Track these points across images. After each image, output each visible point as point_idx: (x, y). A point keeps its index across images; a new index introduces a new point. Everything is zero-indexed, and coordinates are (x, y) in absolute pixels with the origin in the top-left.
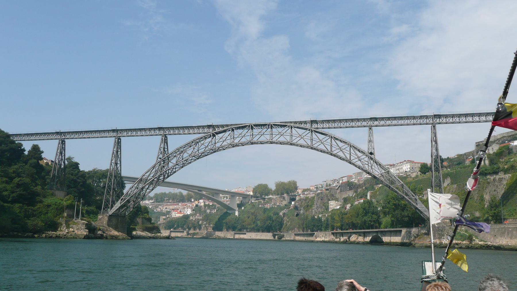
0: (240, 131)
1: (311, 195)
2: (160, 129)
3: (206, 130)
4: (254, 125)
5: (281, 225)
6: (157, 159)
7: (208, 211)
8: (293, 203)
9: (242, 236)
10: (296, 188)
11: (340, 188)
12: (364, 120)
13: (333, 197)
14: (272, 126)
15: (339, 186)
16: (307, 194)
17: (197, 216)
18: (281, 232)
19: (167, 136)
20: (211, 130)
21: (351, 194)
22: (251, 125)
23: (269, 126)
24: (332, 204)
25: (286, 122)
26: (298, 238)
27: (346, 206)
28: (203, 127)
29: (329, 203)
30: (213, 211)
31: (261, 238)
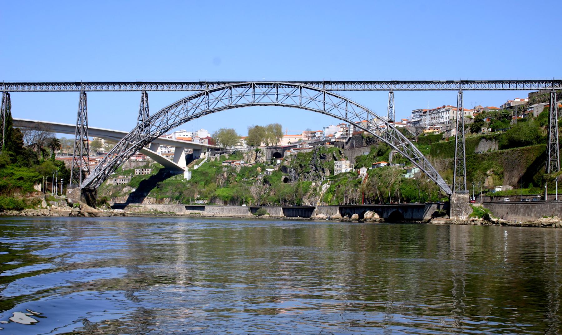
0: (240, 90)
3: (197, 87)
4: (256, 84)
6: (138, 123)
7: (138, 171)
15: (350, 139)
16: (300, 149)
17: (119, 180)
19: (146, 92)
20: (203, 88)
22: (253, 83)
23: (275, 85)
27: (360, 170)
29: (335, 163)
30: (146, 172)
31: (229, 214)
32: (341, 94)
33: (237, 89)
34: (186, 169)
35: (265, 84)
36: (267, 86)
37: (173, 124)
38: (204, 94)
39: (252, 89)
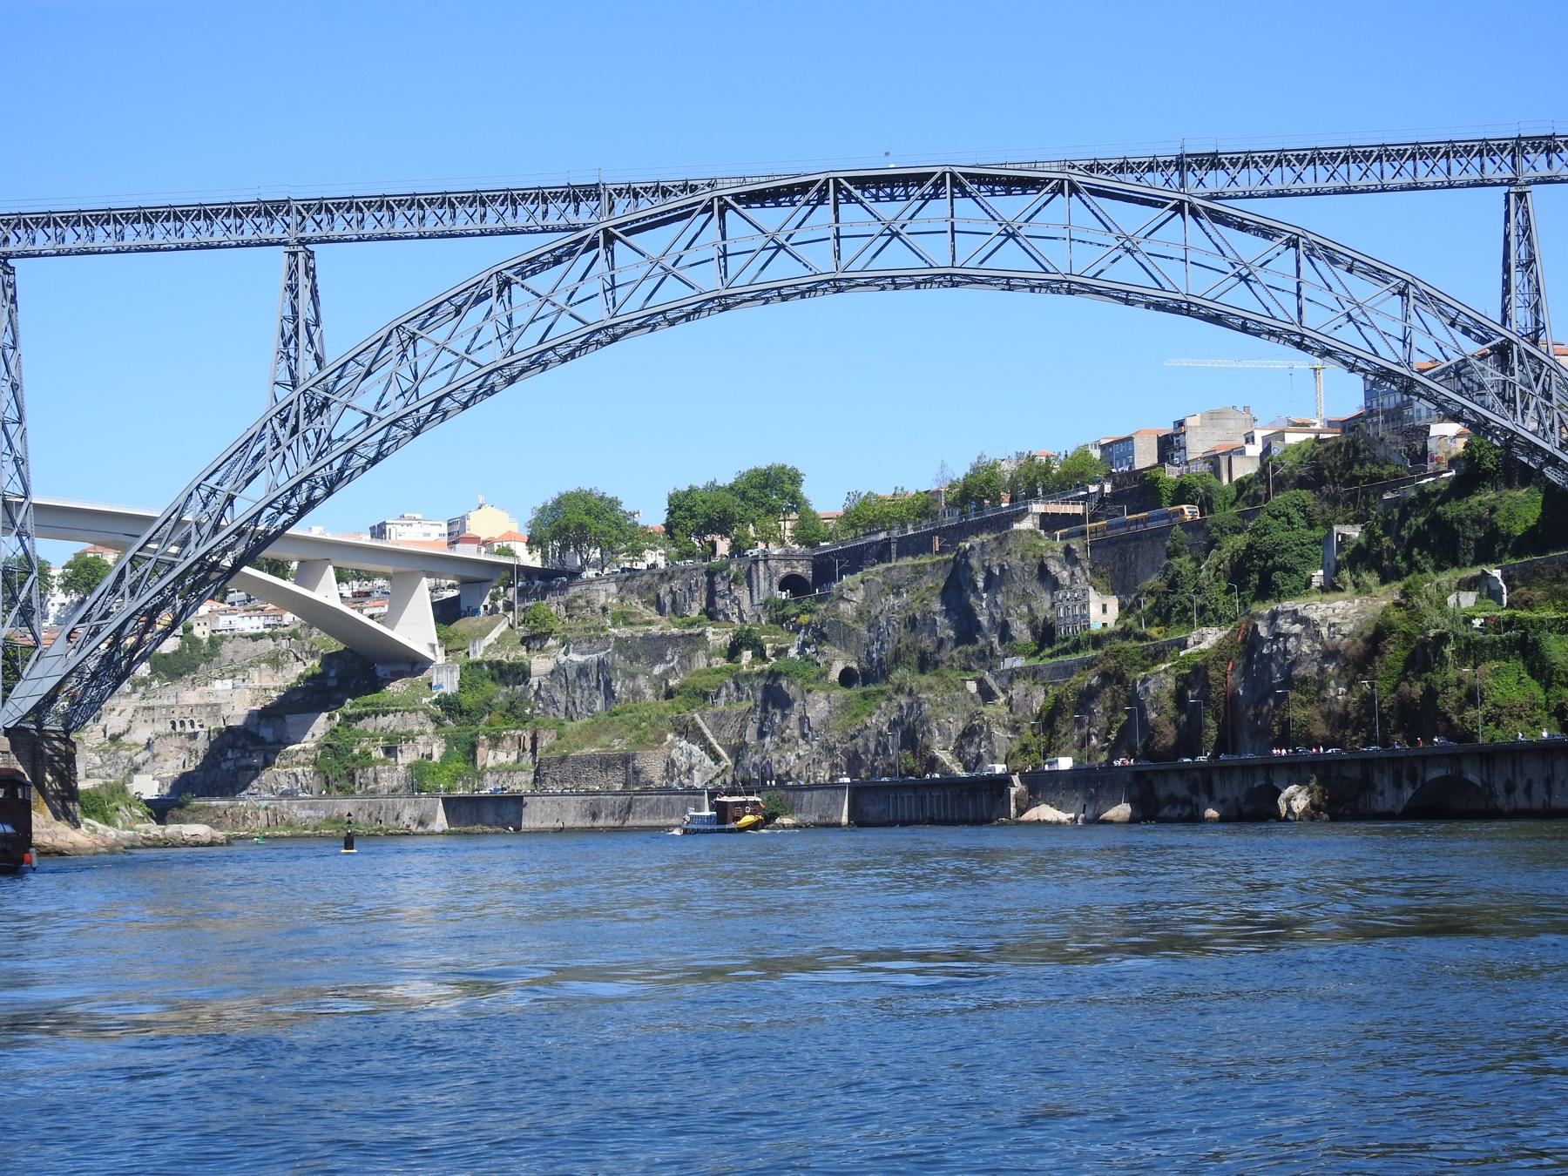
0: (770, 217)
2: (270, 210)
4: (849, 180)
28: (542, 197)
33: (755, 213)
34: (440, 658)
35: (891, 181)
36: (899, 191)
37: (448, 394)
38: (594, 244)
39: (825, 212)
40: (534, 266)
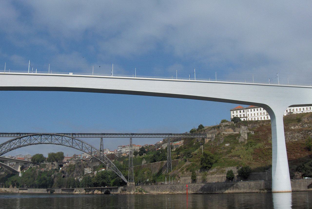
0: (35, 137)
1: (74, 163)
3: (16, 135)
5: (52, 182)
8: (61, 169)
9: (24, 191)
10: (63, 157)
11: (92, 160)
12: (99, 134)
13: (87, 166)
14: (52, 135)
15: (91, 158)
18: (53, 188)
20: (18, 135)
21: (98, 164)
24: (86, 170)
25: (59, 134)
26: (63, 192)
28: (14, 134)
32: (80, 139)
33: (34, 136)
34: (20, 172)
35: (46, 134)
40: (13, 140)
